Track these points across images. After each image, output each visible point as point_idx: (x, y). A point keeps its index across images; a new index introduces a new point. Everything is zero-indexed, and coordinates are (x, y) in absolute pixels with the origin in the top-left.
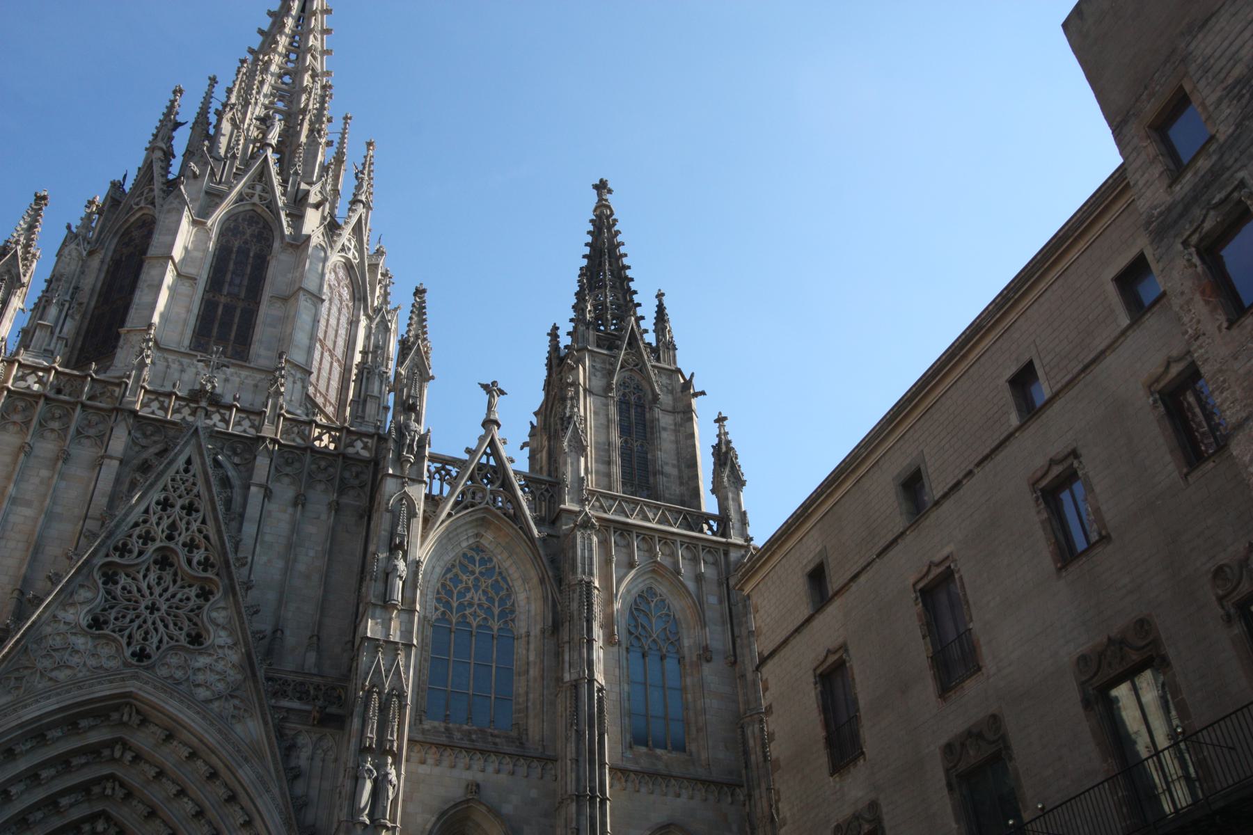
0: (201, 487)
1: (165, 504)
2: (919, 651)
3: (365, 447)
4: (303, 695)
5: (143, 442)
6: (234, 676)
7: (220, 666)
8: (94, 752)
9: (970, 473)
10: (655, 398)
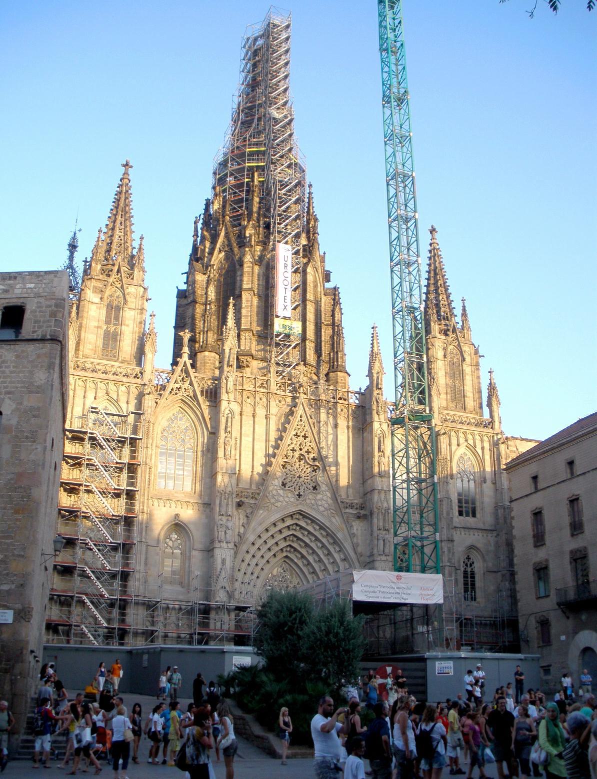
0: (307, 428)
1: (296, 435)
2: (566, 520)
3: (357, 399)
4: (351, 506)
5: (280, 405)
6: (330, 501)
7: (325, 498)
8: (288, 527)
9: (589, 472)
10: (464, 360)
